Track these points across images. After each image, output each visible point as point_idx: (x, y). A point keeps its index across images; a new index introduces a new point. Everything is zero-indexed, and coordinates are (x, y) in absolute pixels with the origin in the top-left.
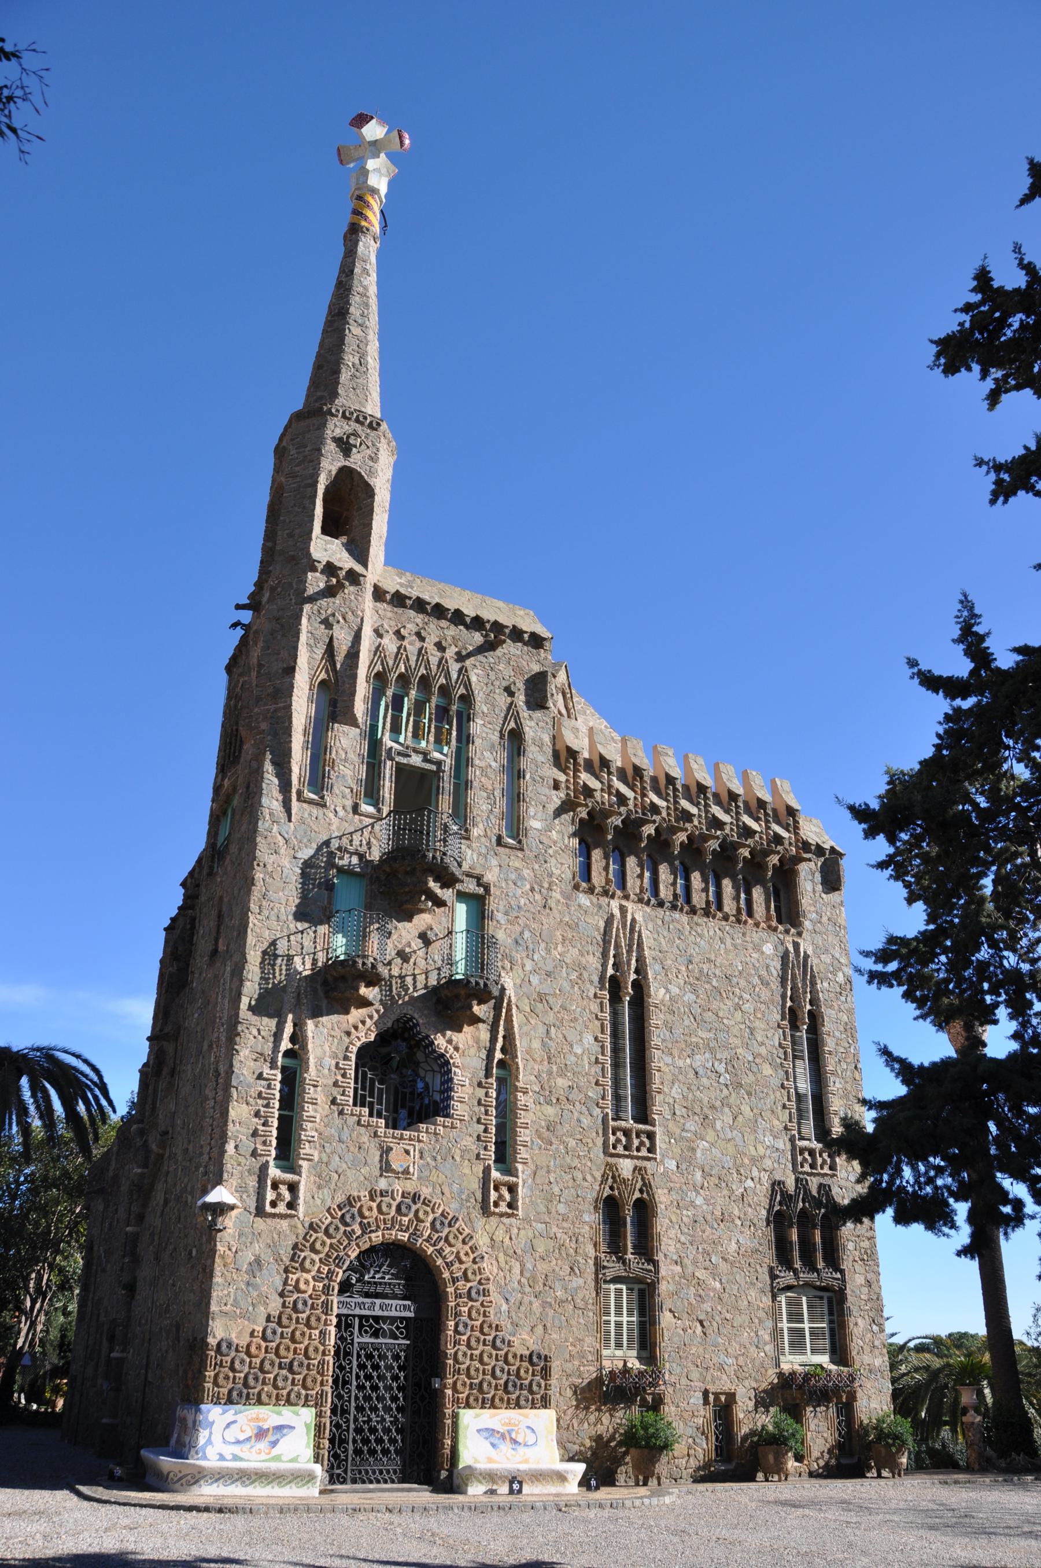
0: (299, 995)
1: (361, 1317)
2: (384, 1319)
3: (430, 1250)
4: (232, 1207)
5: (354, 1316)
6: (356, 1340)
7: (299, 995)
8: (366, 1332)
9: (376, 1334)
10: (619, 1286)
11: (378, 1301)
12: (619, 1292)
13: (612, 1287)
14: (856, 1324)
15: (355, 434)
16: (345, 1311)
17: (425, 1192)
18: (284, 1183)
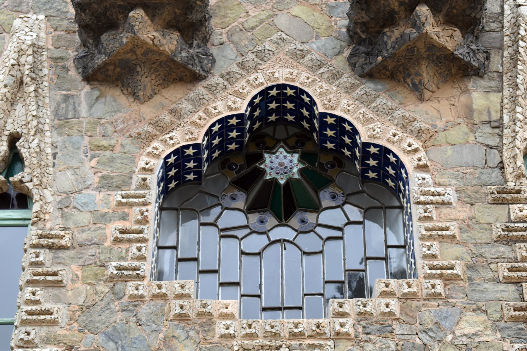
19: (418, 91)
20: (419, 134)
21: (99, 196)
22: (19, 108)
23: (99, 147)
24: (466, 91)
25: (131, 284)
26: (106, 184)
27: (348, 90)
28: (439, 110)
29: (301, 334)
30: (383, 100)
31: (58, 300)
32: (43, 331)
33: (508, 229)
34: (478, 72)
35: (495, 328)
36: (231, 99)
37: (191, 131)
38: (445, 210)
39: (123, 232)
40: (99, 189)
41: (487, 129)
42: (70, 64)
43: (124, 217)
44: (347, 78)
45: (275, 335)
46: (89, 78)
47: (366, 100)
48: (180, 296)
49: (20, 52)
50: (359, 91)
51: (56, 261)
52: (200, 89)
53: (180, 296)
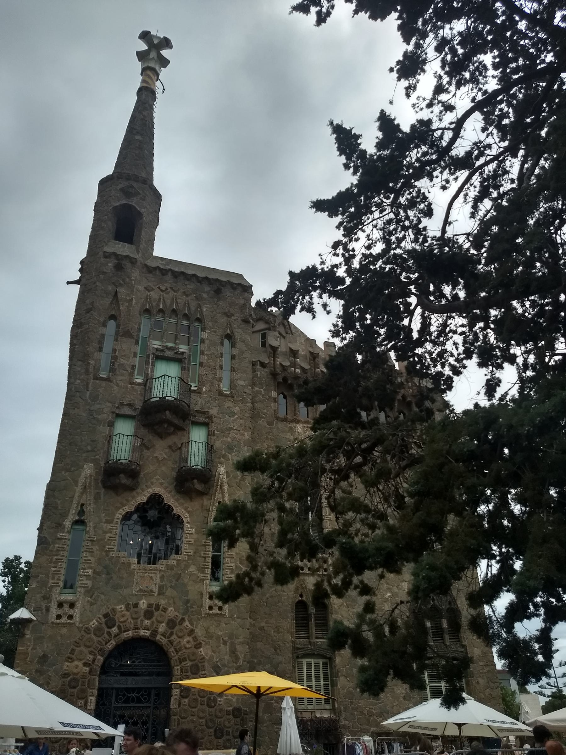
0: (85, 487)
1: (117, 689)
2: (133, 690)
3: (164, 641)
4: (29, 621)
5: (112, 689)
6: (113, 705)
7: (85, 487)
8: (121, 699)
9: (126, 701)
10: (309, 660)
11: (130, 678)
12: (309, 664)
13: (305, 661)
14: (478, 682)
15: (132, 187)
16: (105, 686)
17: (163, 602)
18: (66, 602)
19: (191, 499)
20: (189, 512)
21: (105, 525)
22: (84, 496)
23: (105, 510)
24: (203, 500)
25: (111, 553)
26: (107, 522)
27: (173, 497)
28: (195, 505)
29: (152, 570)
30: (182, 501)
31: (92, 556)
32: (88, 565)
33: (205, 542)
34: (206, 494)
35: (198, 570)
36: (142, 498)
37: (130, 507)
38: (192, 535)
39: (110, 537)
40: (104, 523)
41: (206, 512)
42: (99, 481)
43: (111, 532)
44: (173, 493)
45: (145, 570)
46: (105, 487)
47: (177, 500)
48: (123, 557)
49: (86, 478)
50: (176, 497)
51: (92, 545)
52: (134, 493)
53: (123, 557)
